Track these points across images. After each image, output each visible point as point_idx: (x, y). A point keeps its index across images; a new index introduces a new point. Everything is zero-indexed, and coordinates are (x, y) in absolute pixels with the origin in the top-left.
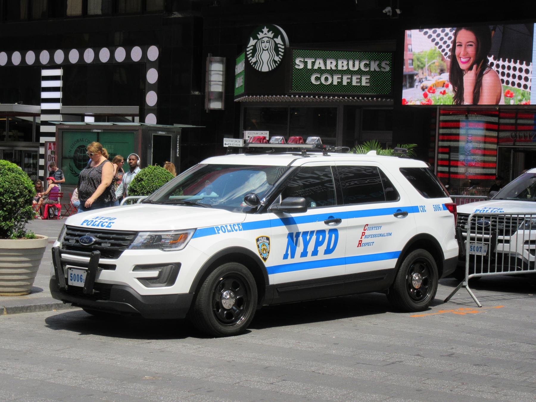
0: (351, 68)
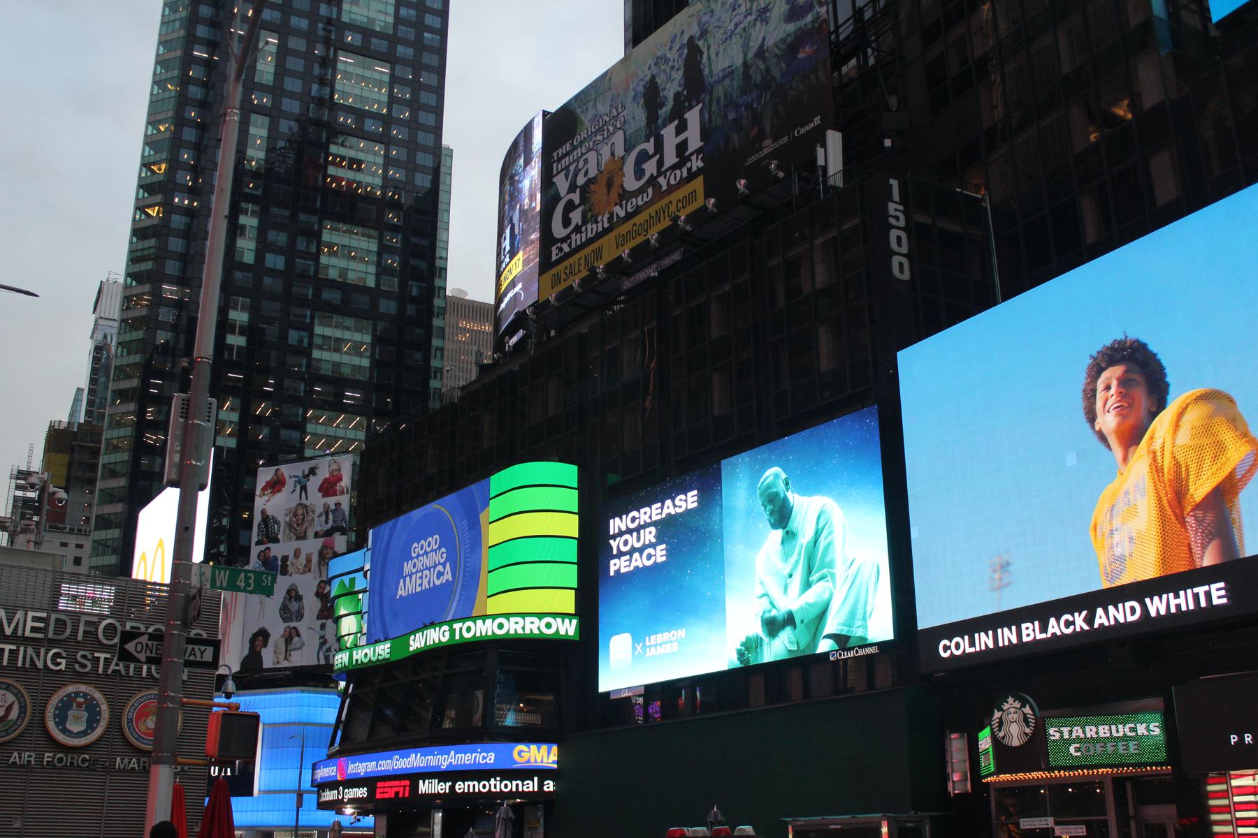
0: (1115, 734)
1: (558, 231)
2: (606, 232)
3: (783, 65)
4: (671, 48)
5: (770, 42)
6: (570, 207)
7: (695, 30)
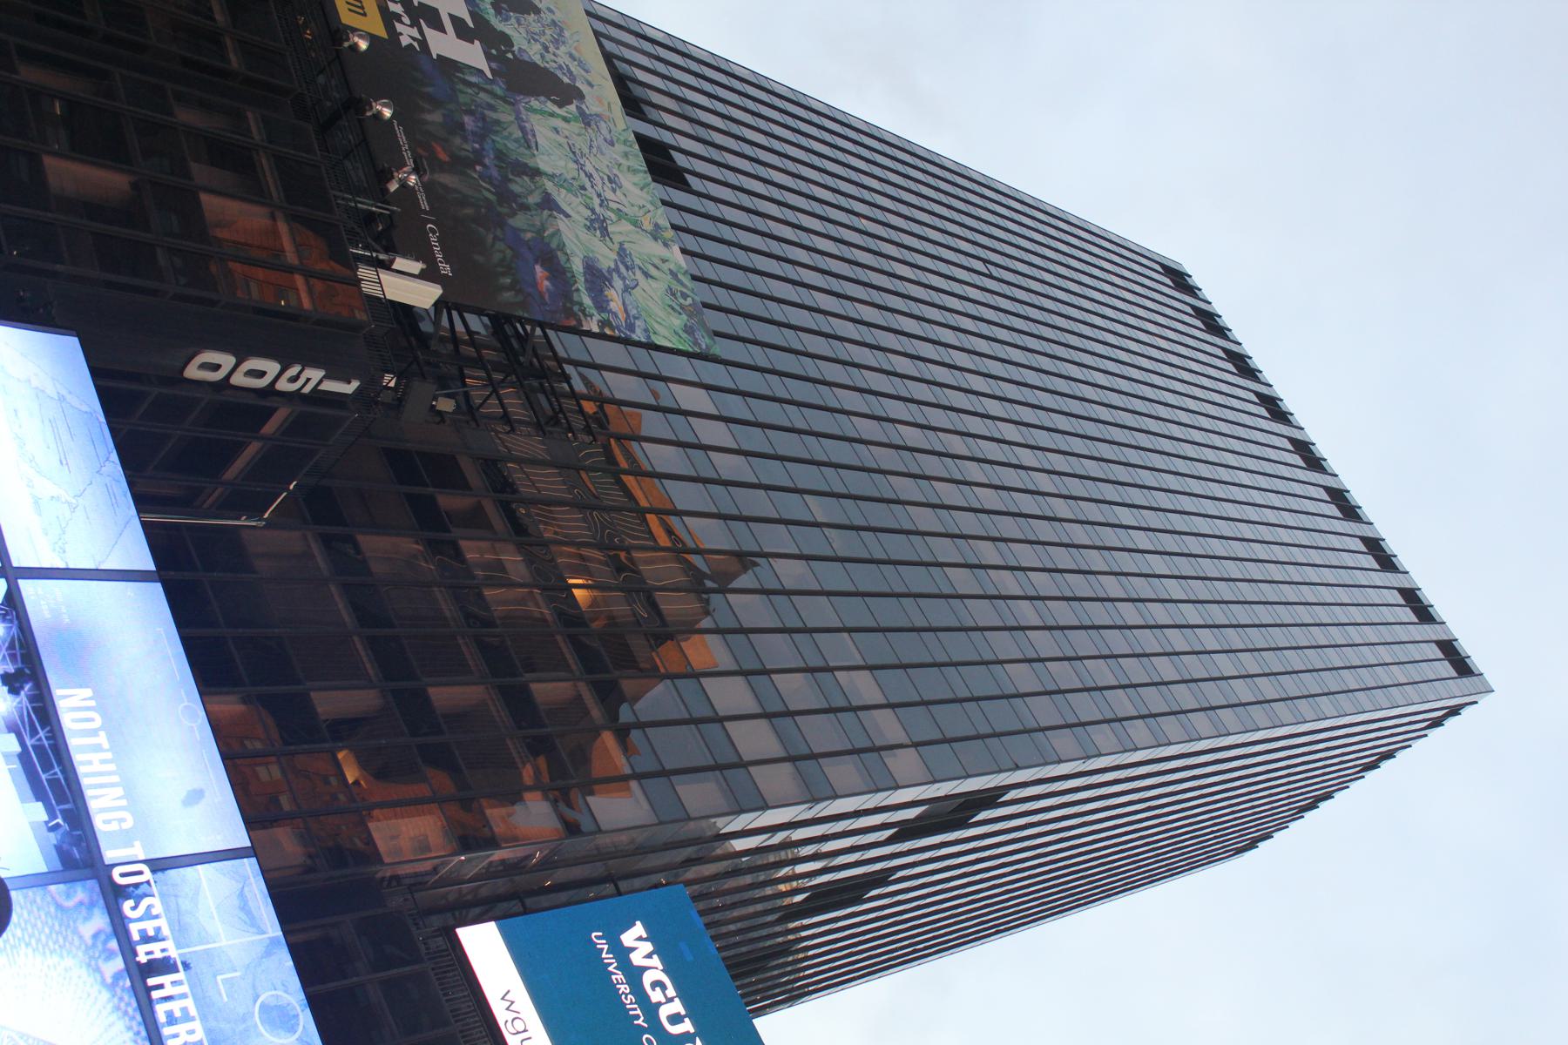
3: (529, 235)
4: (571, 56)
5: (562, 224)
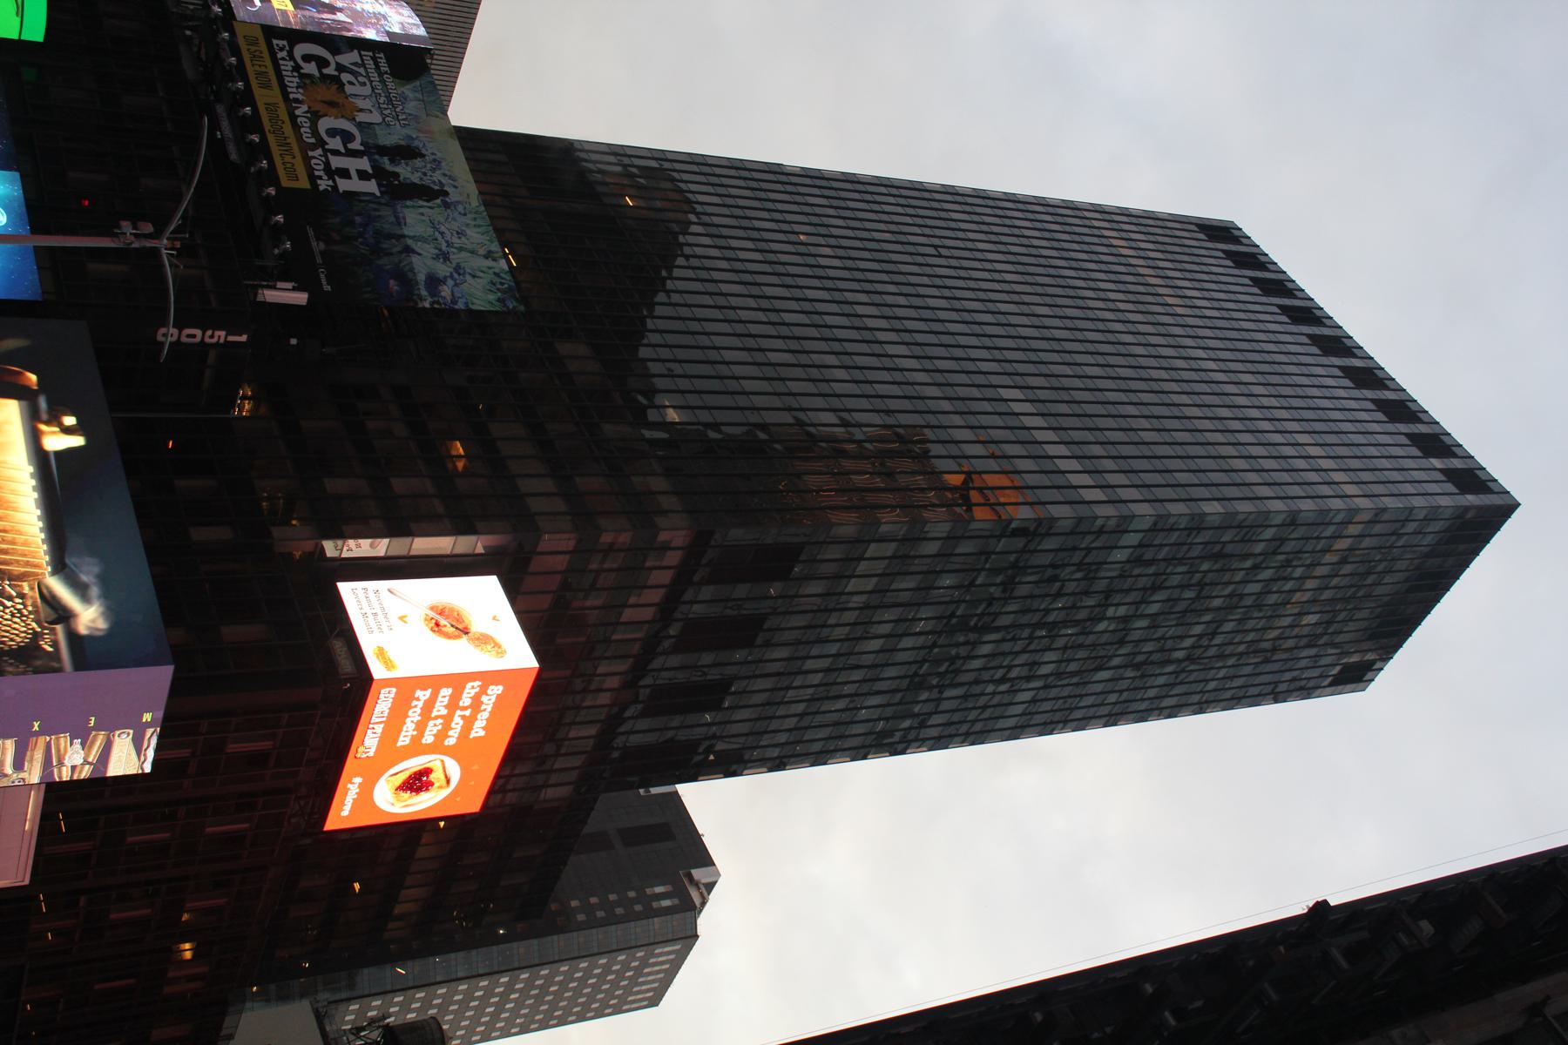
1: (301, 49)
2: (285, 94)
5: (415, 259)
6: (322, 63)
7: (454, 196)
